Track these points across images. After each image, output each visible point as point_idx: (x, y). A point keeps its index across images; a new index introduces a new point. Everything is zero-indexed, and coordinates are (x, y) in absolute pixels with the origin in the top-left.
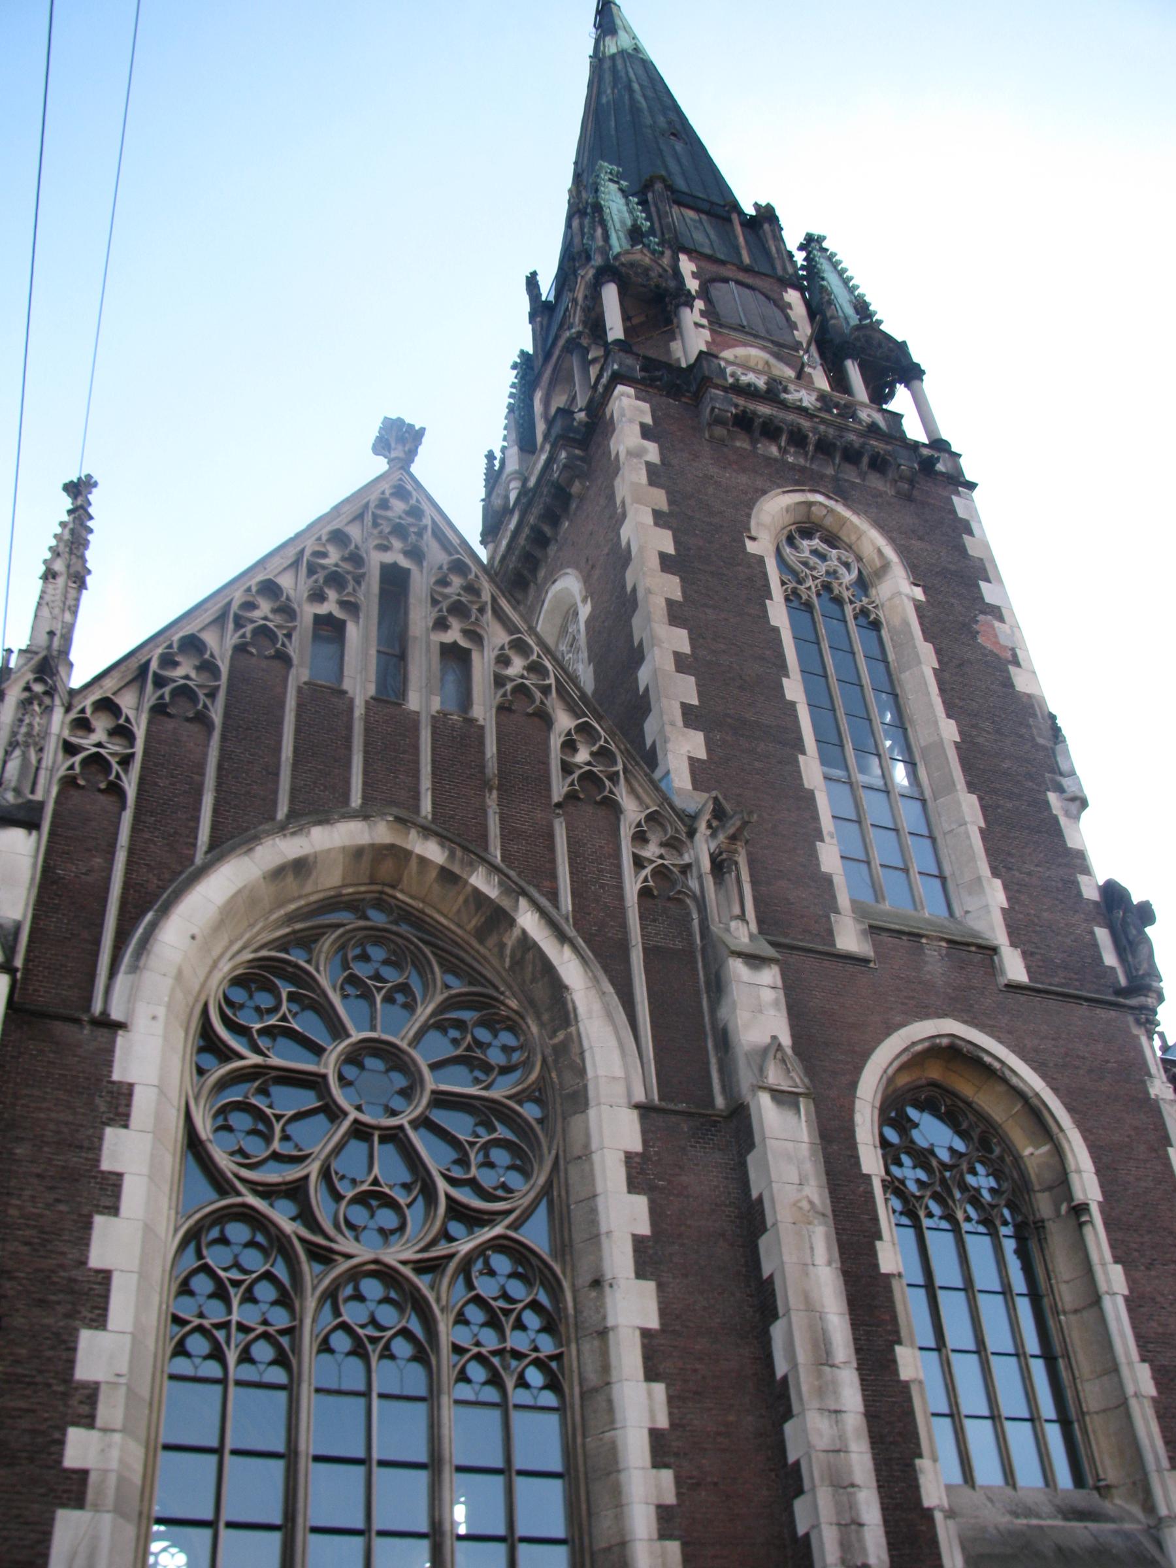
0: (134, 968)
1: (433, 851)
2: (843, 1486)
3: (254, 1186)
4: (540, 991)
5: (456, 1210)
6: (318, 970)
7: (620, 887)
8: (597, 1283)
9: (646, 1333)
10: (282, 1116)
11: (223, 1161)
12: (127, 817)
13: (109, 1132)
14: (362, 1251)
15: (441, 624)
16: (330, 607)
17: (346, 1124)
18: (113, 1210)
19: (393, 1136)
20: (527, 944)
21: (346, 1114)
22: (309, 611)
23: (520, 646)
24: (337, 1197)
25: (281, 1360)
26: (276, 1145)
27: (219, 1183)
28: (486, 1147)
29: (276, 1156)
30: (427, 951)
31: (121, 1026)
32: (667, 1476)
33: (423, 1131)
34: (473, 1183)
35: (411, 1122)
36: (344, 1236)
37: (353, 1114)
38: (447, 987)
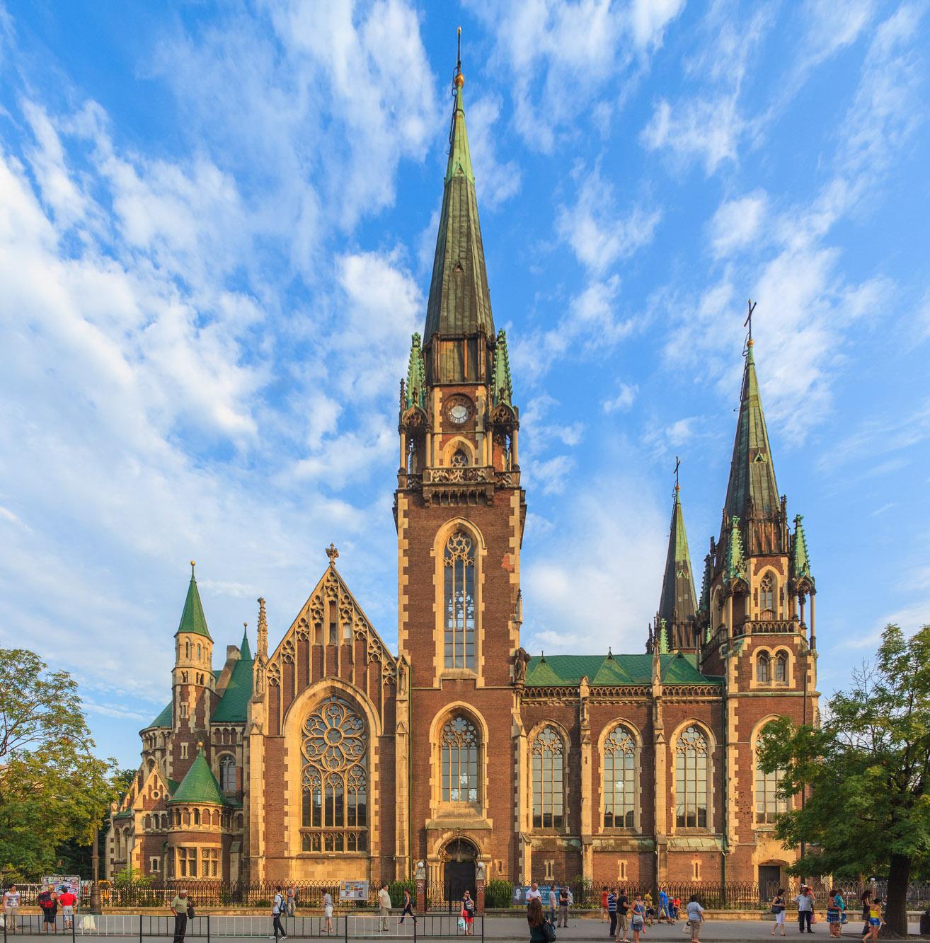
2: (401, 809)
3: (313, 761)
5: (348, 760)
13: (285, 757)
14: (331, 770)
18: (287, 771)
19: (337, 747)
21: (327, 745)
37: (329, 744)
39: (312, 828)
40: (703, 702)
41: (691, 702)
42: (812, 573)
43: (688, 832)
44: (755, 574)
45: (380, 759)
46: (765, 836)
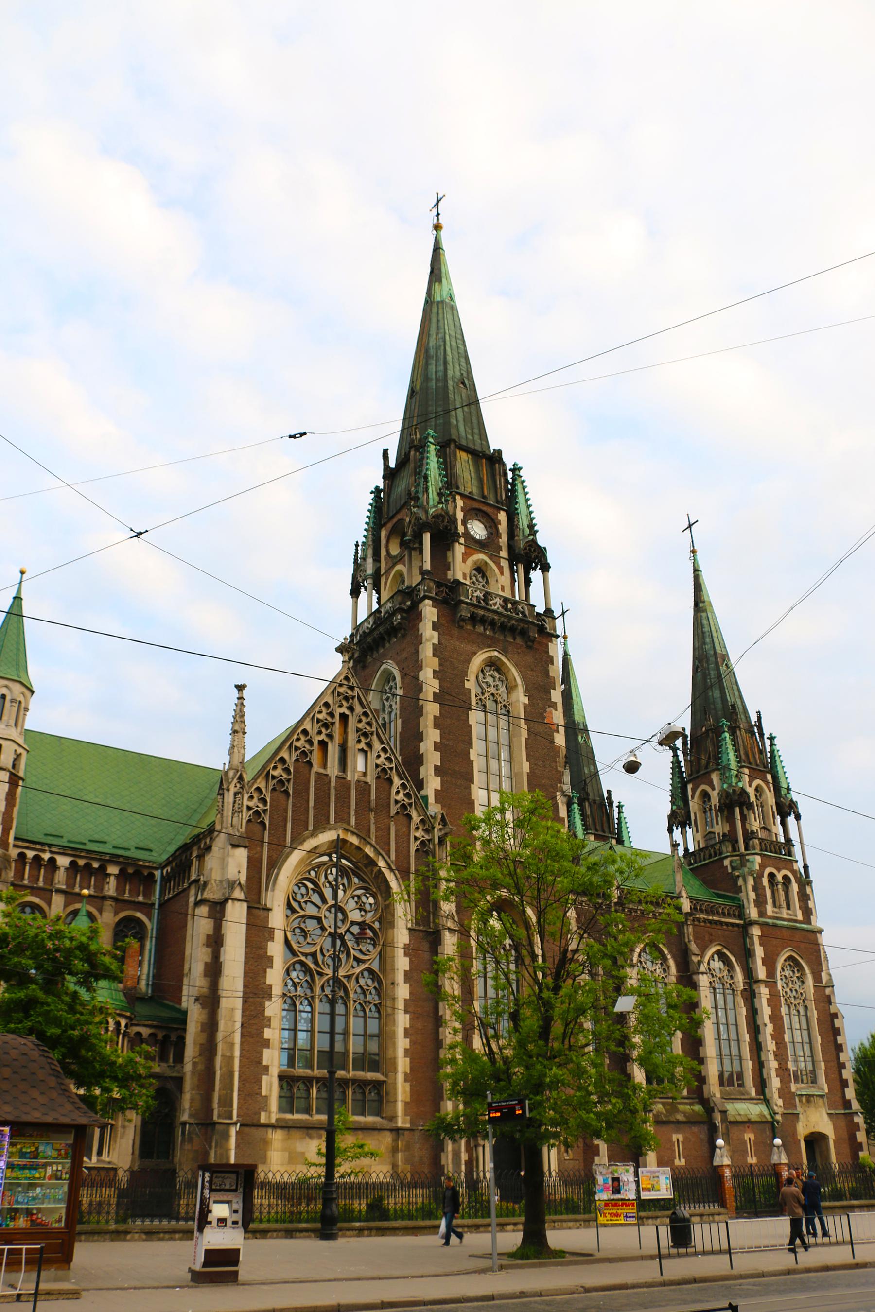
0: (273, 890)
1: (354, 840)
4: (383, 888)
5: (356, 958)
7: (409, 847)
8: (393, 984)
9: (405, 1000)
11: (295, 946)
12: (267, 833)
15: (359, 741)
16: (322, 737)
18: (271, 967)
20: (380, 872)
22: (316, 739)
23: (384, 750)
24: (324, 956)
25: (310, 1005)
27: (293, 953)
31: (269, 910)
32: (408, 1040)
34: (360, 950)
39: (300, 1071)
40: (727, 924)
41: (716, 922)
42: (795, 797)
43: (729, 1094)
44: (750, 786)
45: (411, 962)
46: (804, 1099)
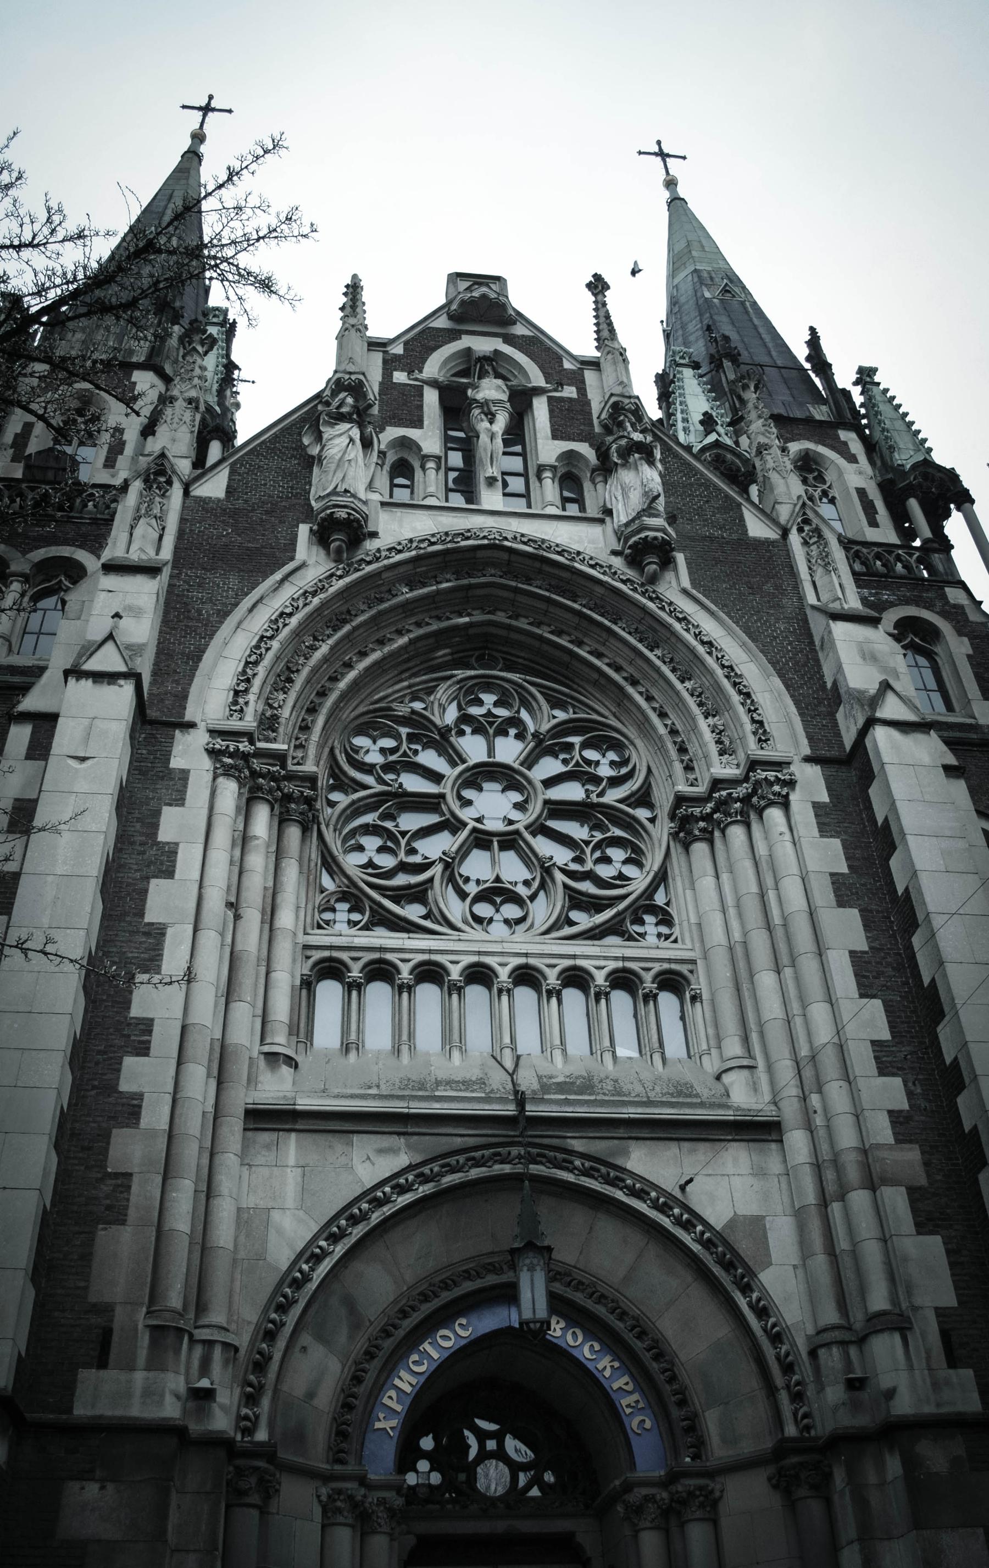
6: (433, 715)
10: (408, 831)
17: (466, 832)
19: (510, 841)
24: (463, 895)
26: (402, 855)
28: (598, 846)
29: (403, 867)
30: (533, 689)
33: (540, 838)
34: (589, 876)
35: (527, 828)
36: (473, 928)
37: (472, 824)
38: (554, 717)
